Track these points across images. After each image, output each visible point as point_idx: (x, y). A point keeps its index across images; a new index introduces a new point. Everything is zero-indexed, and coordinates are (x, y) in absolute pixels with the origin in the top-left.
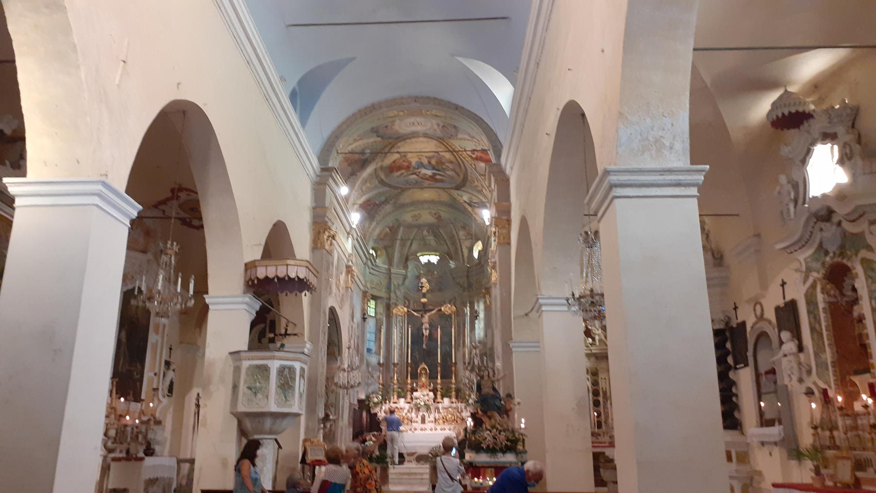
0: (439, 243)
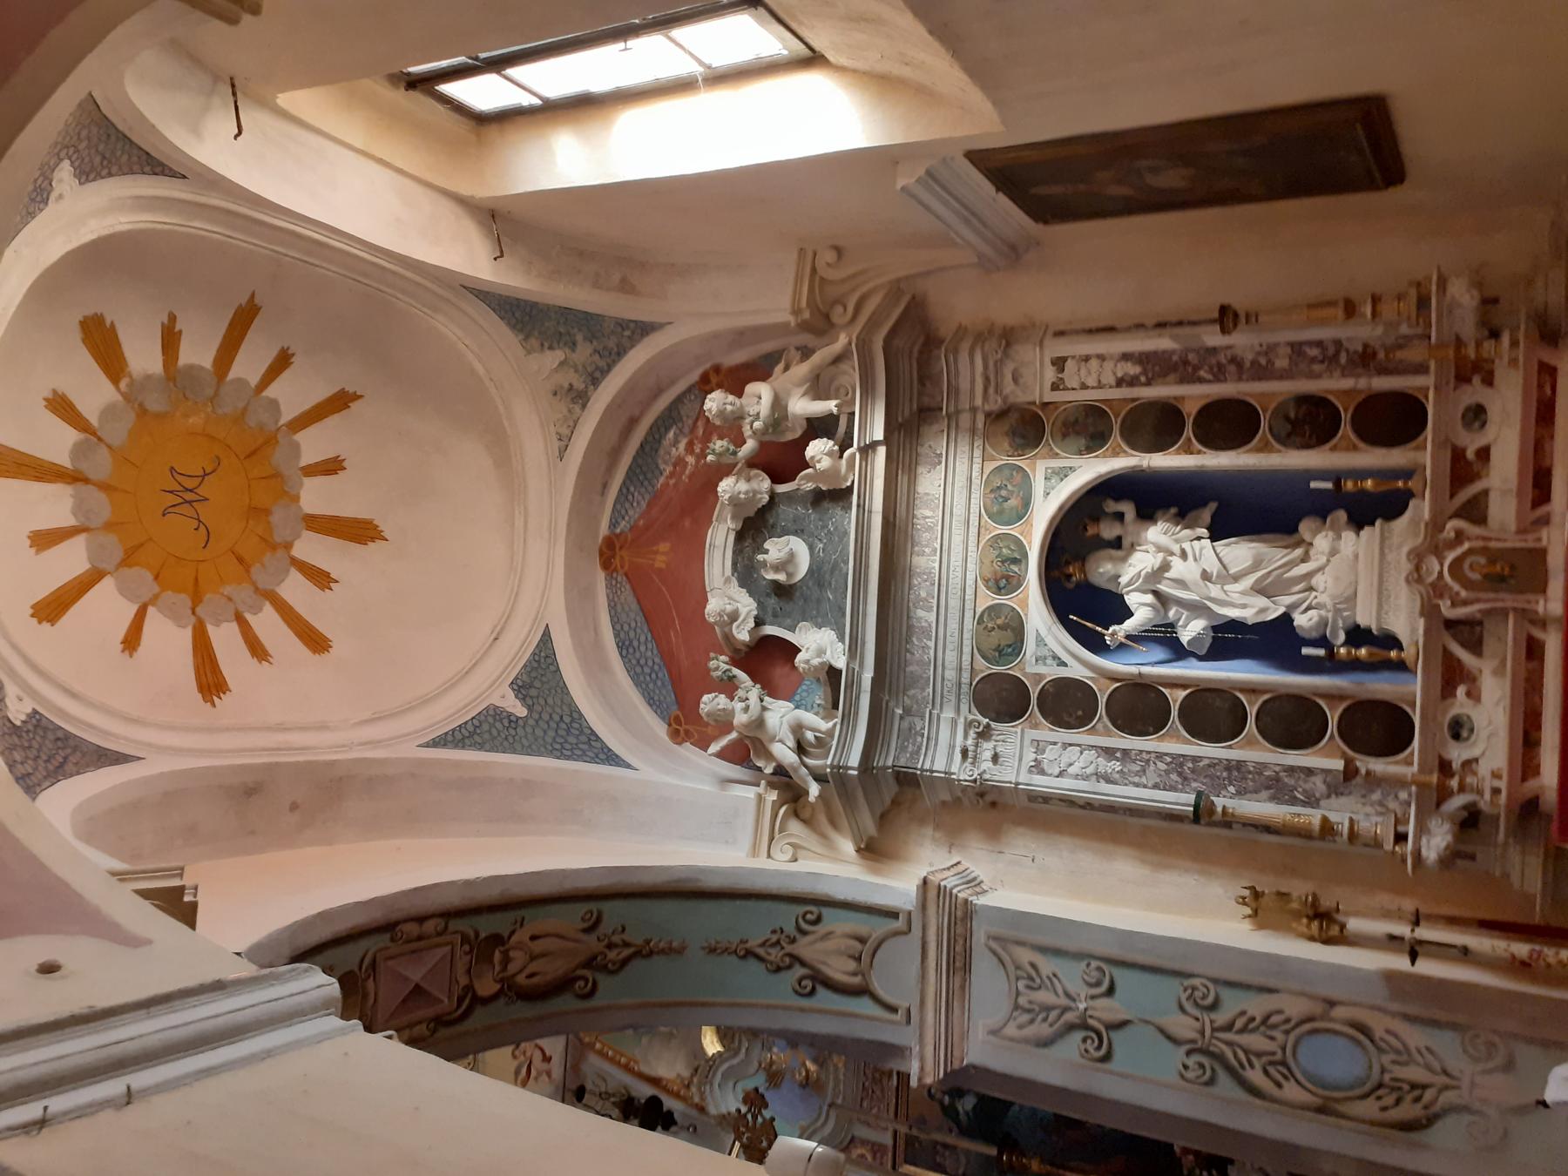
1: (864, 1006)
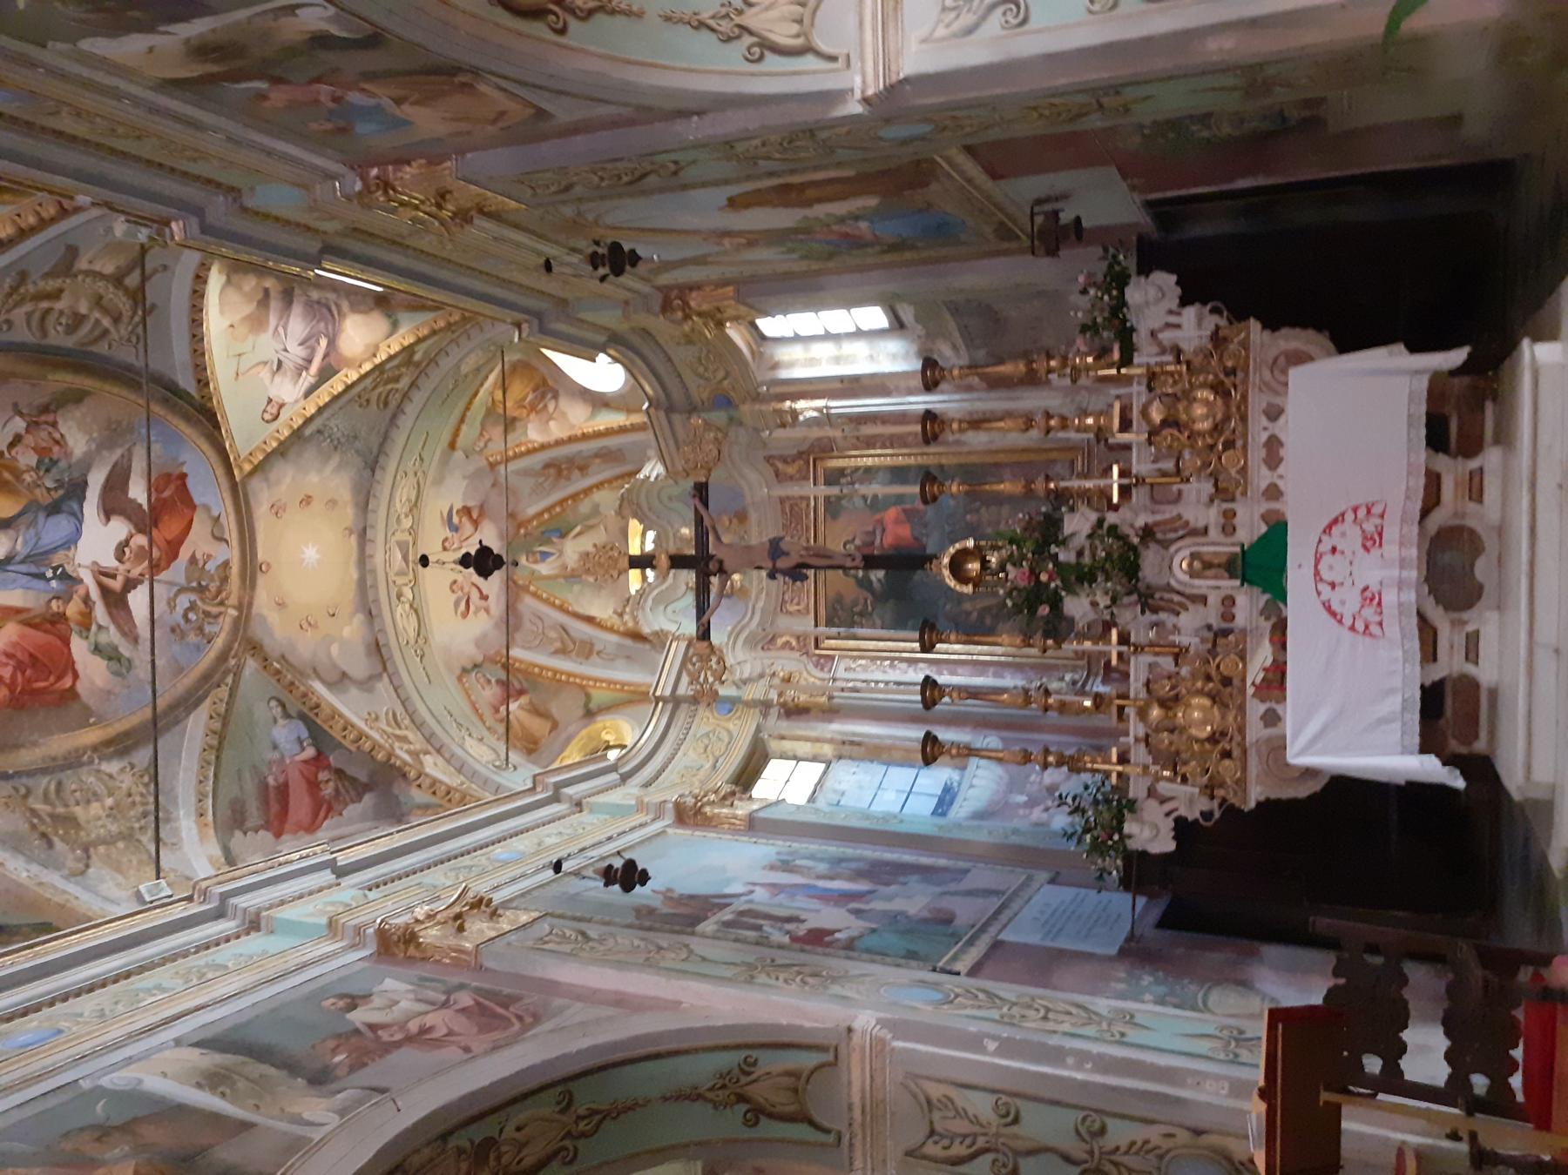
0: (591, 522)
1: (810, 62)
